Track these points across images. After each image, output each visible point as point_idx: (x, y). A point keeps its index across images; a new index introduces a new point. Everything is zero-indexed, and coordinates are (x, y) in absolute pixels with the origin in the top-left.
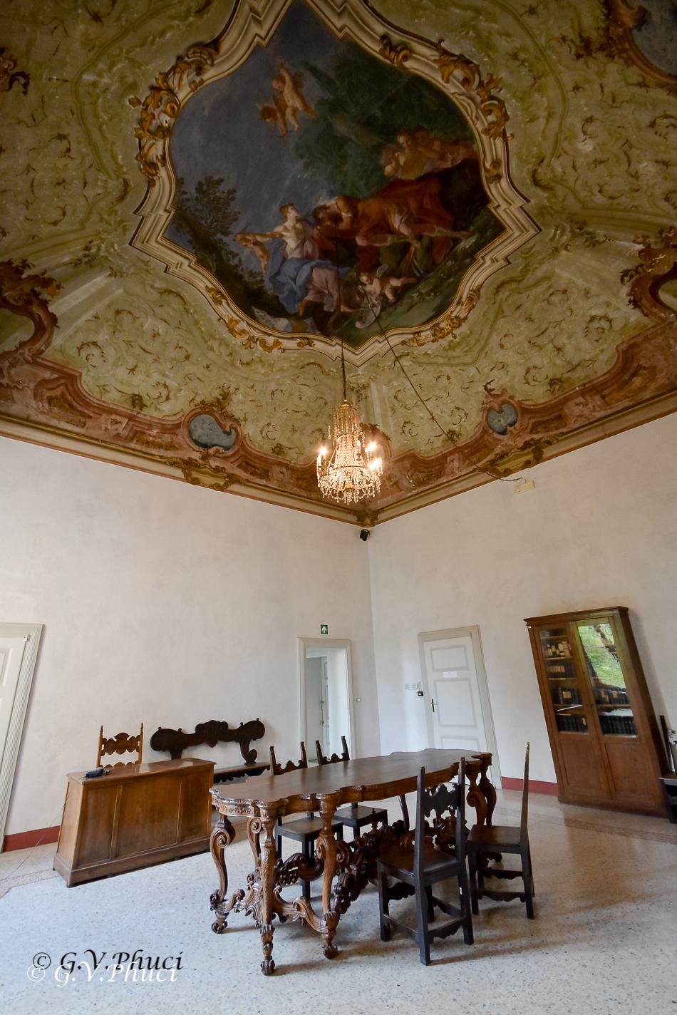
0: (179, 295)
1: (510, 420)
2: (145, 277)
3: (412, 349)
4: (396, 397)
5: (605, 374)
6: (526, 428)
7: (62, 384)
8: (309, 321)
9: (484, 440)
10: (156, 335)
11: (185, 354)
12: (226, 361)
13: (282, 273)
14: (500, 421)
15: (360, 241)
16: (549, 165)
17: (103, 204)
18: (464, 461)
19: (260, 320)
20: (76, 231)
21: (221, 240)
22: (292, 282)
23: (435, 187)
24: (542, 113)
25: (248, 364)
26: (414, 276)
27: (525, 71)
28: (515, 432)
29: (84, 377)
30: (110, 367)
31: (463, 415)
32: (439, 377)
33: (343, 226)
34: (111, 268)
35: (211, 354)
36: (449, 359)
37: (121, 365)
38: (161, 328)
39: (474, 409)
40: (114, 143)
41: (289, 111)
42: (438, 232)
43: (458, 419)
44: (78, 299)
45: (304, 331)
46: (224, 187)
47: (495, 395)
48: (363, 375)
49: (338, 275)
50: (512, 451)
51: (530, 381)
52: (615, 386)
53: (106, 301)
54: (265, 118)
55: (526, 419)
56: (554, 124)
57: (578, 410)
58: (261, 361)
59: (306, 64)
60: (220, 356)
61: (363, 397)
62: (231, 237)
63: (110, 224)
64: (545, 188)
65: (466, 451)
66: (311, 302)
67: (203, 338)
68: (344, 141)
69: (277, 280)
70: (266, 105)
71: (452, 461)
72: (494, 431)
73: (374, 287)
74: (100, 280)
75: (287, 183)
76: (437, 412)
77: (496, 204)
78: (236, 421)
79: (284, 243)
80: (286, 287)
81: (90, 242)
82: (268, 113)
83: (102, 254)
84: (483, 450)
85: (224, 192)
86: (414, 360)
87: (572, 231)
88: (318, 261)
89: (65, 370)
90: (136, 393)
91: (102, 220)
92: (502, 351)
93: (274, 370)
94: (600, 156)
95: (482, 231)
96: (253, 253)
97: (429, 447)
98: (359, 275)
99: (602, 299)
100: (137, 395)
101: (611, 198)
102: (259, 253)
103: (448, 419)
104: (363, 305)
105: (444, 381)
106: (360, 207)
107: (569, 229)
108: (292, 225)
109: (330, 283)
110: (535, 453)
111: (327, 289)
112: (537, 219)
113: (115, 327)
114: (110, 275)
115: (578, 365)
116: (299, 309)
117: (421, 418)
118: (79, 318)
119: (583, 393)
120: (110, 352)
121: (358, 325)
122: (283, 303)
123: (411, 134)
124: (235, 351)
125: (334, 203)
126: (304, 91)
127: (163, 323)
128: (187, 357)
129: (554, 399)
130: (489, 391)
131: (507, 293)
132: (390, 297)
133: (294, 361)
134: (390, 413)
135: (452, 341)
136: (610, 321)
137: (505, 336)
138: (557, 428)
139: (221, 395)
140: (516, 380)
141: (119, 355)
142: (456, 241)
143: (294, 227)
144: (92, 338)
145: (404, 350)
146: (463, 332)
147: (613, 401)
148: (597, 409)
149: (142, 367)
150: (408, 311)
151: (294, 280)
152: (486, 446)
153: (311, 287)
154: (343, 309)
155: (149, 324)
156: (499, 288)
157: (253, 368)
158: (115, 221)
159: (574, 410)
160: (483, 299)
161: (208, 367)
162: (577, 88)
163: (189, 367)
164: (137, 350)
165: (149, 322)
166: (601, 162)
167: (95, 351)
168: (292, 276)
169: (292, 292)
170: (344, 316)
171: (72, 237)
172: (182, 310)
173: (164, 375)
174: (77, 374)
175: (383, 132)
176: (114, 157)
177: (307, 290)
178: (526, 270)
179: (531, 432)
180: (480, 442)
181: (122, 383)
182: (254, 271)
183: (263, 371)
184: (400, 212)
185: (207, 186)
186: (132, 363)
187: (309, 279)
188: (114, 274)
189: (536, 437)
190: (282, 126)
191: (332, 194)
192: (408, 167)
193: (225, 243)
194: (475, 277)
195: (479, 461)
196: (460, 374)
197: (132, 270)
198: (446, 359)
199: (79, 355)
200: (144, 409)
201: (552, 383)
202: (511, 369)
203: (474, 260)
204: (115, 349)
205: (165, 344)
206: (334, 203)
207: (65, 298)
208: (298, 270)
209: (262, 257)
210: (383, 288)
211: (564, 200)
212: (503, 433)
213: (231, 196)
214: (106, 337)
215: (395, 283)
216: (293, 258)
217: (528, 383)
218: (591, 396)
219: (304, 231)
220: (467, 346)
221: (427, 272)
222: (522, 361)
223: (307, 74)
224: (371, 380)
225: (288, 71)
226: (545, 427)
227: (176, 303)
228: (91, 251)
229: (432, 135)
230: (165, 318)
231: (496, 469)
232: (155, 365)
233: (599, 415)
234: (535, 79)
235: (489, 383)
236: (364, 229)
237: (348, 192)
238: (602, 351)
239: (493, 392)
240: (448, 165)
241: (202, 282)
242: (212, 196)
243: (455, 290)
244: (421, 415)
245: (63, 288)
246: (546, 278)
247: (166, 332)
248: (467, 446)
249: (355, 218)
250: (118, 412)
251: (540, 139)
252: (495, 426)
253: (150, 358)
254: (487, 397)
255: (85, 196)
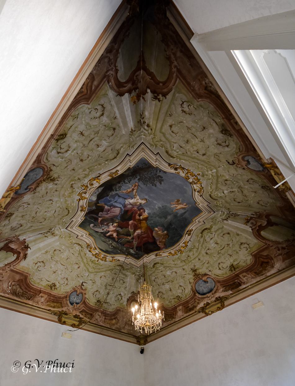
0: (115, 158)
1: (78, 301)
2: (127, 145)
3: (86, 248)
4: (55, 250)
5: (110, 312)
6: (80, 309)
7: (87, 92)
8: (94, 208)
9: (63, 300)
10: (98, 146)
11: (84, 159)
12: (75, 177)
13: (120, 198)
14: (74, 298)
15: (131, 222)
16: (161, 266)
17: (168, 146)
18: (47, 302)
19: (97, 190)
20: (161, 128)
21: (137, 177)
22: (115, 201)
23: (150, 241)
24: (175, 263)
25: (72, 187)
26: (118, 240)
27: (186, 258)
28: (76, 307)
29: (86, 106)
30: (87, 121)
31: (66, 283)
32: (77, 264)
33: (137, 217)
34: (135, 131)
35: (81, 170)
36: (87, 263)
37: (86, 127)
38: (101, 149)
39: (71, 285)
40: (190, 163)
41: (177, 205)
42: (135, 243)
43: (63, 282)
44: (127, 111)
45: (89, 206)
46: (158, 184)
47: (82, 288)
48: (61, 232)
49: (117, 216)
50: (70, 314)
51: (94, 295)
52: (109, 318)
53: (121, 125)
54: (177, 200)
55: (82, 306)
56: (173, 266)
57: (97, 317)
58: (73, 192)
59: (188, 211)
60: (79, 175)
61: (46, 235)
62: (138, 181)
63: (157, 141)
64: (154, 266)
65: (52, 298)
66: (104, 208)
67: (91, 167)
68: (166, 218)
69: (116, 196)
70: (180, 201)
71: (42, 297)
72: (69, 300)
73: (112, 228)
74: (131, 124)
75: (155, 202)
76: (59, 272)
77: (147, 257)
78: (35, 189)
79: (132, 198)
80: (112, 199)
81: (151, 130)
82: (178, 201)
83: (142, 129)
84: (59, 304)
85: (156, 183)
86: (80, 251)
87: (140, 274)
88: (123, 209)
89: (94, 95)
90: (67, 136)
91: (161, 141)
92: (99, 279)
93: (66, 198)
94: (166, 276)
95: (137, 254)
96: (129, 188)
97: (38, 281)
98: (116, 223)
99: (126, 292)
100: (66, 136)
101: (154, 281)
102: (129, 190)
103: (59, 279)
104: (102, 225)
105: (77, 266)
106: (144, 221)
107: (140, 273)
108: (139, 202)
109: (113, 214)
110: (79, 324)
111: (110, 213)
112: (144, 266)
113: (108, 126)
114: (132, 130)
115: (107, 303)
116: (101, 204)
117: (51, 268)
118: (118, 109)
119: (102, 313)
120: (95, 122)
121: (92, 225)
122: (105, 198)
123: (167, 234)
124: (81, 181)
125: (146, 214)
126: (181, 210)
127: (103, 150)
128: (82, 160)
129: (95, 307)
130: (82, 285)
131: (119, 268)
132: (108, 234)
133: (71, 205)
134: (43, 251)
135: (95, 261)
136: (122, 299)
137: (105, 276)
138: (89, 318)
139: (54, 178)
140: (92, 290)
141: (92, 127)
142: (132, 249)
143: (138, 202)
144: (106, 113)
145: (85, 246)
146: (100, 262)
147: (106, 323)
148: (102, 321)
149: (82, 138)
150: (103, 241)
151: (116, 202)
152: (61, 303)
153: (112, 207)
154: (100, 219)
155: (105, 143)
156: (120, 265)
157: (69, 189)
158: (157, 144)
159: (98, 317)
160: (114, 263)
161: (73, 170)
162: (184, 269)
163: (75, 162)
164: (92, 136)
165: (106, 143)
166: (165, 277)
167: (99, 114)
168: (117, 201)
169: (110, 201)
170: (96, 219)
171: (159, 125)
172: (108, 159)
173: (74, 150)
174: (89, 102)
175: (168, 227)
176: (185, 160)
177: (110, 206)
178: (127, 269)
179: (80, 312)
180: (61, 299)
181: (76, 127)
182: (121, 188)
183: (66, 194)
184: (141, 232)
185: (161, 180)
186: (86, 133)
187: (115, 207)
188: (132, 131)
189: (81, 316)
190: (174, 203)
191: (149, 214)
192: (157, 233)
193: (135, 179)
194: (121, 258)
195: (54, 307)
196: (83, 271)
197: (131, 140)
198: (87, 262)
199: (99, 105)
200: (56, 141)
201: (98, 301)
202: (95, 285)
203: (127, 255)
204: (96, 125)
205: (92, 150)
206: (146, 214)
207: (129, 105)
208: (120, 203)
209: (127, 191)
210: (112, 231)
211: (150, 271)
212: (72, 304)
213: (154, 185)
214: (104, 121)
215: (115, 235)
216: (126, 201)
217: (93, 294)
218: (103, 315)
219: (136, 205)
220: (96, 267)
221: (121, 243)
222: (99, 287)
223: (185, 211)
224: (59, 236)
225: (187, 207)
226: (85, 315)
227: (111, 156)
228: (146, 126)
229: (167, 239)
230: (106, 151)
231: (61, 318)
232: (82, 145)
233: (101, 324)
234: (184, 261)
235: (85, 282)
236: (135, 223)
237: (149, 218)
238: (114, 304)
239: (82, 286)
240: (158, 243)
241: (121, 170)
242: (156, 179)
243: (115, 254)
244: (53, 266)
245: (133, 105)
246: (126, 276)
247: (98, 151)
248: (54, 296)
249: (140, 220)
250: (59, 127)
251: (168, 263)
252: (71, 299)
253: (86, 143)
254: (79, 286)
255: (175, 143)
